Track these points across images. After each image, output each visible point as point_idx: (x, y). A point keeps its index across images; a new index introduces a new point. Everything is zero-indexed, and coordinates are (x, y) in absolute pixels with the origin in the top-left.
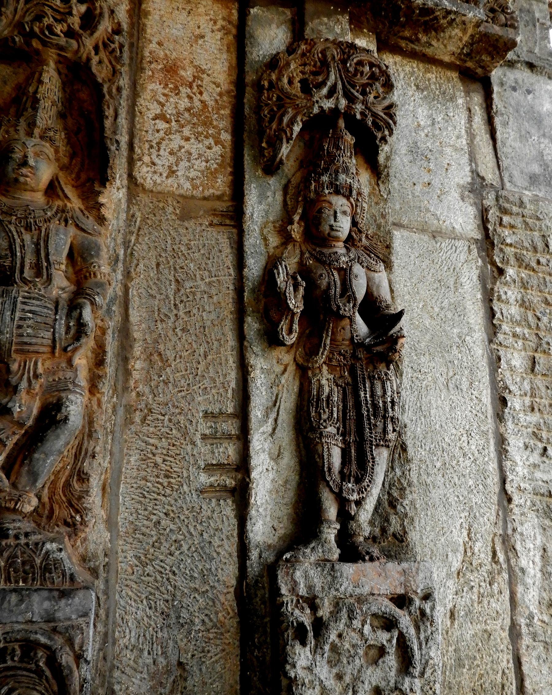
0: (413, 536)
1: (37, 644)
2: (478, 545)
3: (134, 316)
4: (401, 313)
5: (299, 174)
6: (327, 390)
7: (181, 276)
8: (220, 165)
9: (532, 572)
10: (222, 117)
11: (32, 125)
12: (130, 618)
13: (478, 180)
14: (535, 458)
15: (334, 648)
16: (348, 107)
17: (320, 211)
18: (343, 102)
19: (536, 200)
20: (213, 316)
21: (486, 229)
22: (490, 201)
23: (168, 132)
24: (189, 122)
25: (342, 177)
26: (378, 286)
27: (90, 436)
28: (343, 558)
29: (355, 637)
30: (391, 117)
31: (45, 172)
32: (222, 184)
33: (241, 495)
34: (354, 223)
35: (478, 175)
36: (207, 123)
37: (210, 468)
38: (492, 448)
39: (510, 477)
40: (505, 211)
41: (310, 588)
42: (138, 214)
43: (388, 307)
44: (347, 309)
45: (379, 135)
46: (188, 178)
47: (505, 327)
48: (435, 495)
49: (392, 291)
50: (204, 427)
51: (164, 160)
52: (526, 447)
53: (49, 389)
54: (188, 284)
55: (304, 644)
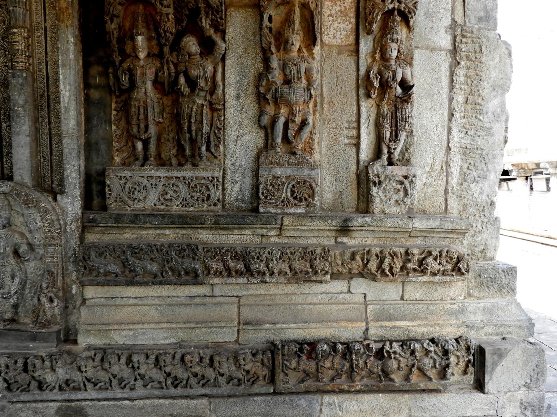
0: (413, 160)
1: (307, 181)
2: (436, 164)
3: (324, 90)
4: (413, 86)
5: (379, 34)
6: (386, 113)
7: (338, 75)
8: (351, 32)
9: (455, 173)
10: (351, 13)
11: (293, 30)
12: (327, 179)
13: (454, 23)
14: (463, 135)
15: (384, 189)
16: (399, 6)
17: (386, 49)
18: (397, 4)
19: (480, 29)
20: (349, 89)
21: (455, 45)
22: (458, 32)
23: (333, 21)
24: (340, 16)
25: (395, 36)
26: (406, 75)
27: (314, 128)
28: (388, 165)
29: (391, 186)
30: (416, 7)
31: (297, 45)
32: (352, 39)
33: (357, 146)
34: (399, 51)
35: (454, 20)
36: (346, 16)
37: (348, 138)
38: (446, 131)
39: (451, 141)
40: (464, 36)
41: (378, 172)
42: (324, 54)
43: (410, 82)
44: (394, 85)
45: (410, 16)
46: (340, 38)
47: (457, 86)
48: (422, 147)
49: (412, 75)
50: (346, 125)
51: (332, 32)
52: (459, 131)
53: (304, 115)
54: (341, 78)
55: (375, 186)
